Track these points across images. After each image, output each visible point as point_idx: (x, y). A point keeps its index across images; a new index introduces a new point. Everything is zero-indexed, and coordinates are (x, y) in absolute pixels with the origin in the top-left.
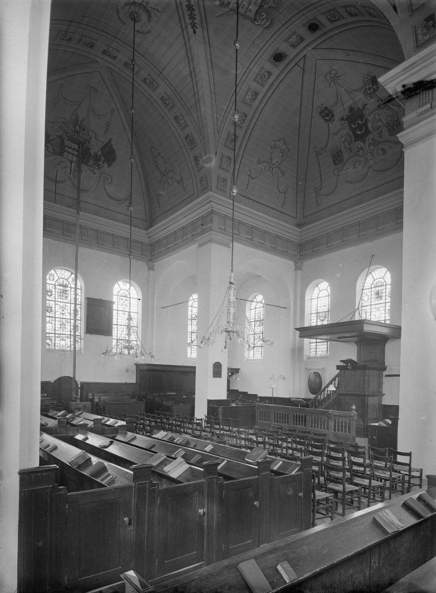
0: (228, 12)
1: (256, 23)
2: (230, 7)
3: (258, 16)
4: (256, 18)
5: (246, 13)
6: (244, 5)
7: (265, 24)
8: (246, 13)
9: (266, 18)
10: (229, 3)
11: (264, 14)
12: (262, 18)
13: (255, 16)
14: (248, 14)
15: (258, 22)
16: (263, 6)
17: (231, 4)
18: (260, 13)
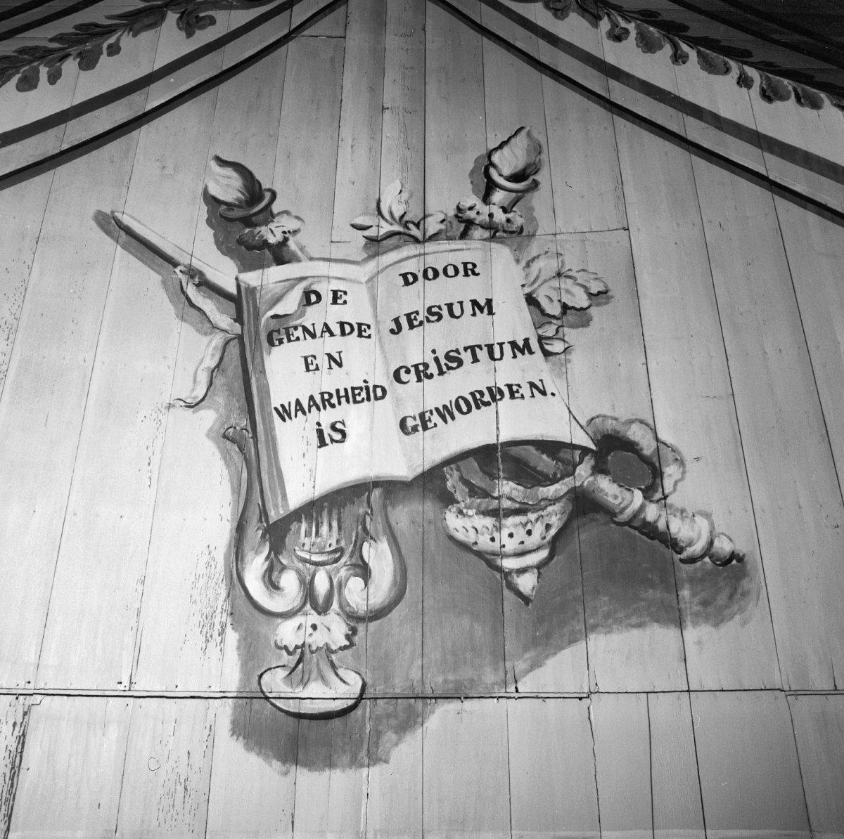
0: (205, 285)
1: (255, 567)
2: (252, 278)
3: (329, 535)
4: (304, 541)
5: (284, 413)
6: (335, 361)
7: (301, 660)
8: (284, 413)
9: (354, 619)
10: (280, 254)
11: (379, 556)
12: (336, 588)
13: (312, 510)
14: (292, 439)
15: (272, 585)
16: (447, 500)
17: (276, 274)
18: (366, 535)
